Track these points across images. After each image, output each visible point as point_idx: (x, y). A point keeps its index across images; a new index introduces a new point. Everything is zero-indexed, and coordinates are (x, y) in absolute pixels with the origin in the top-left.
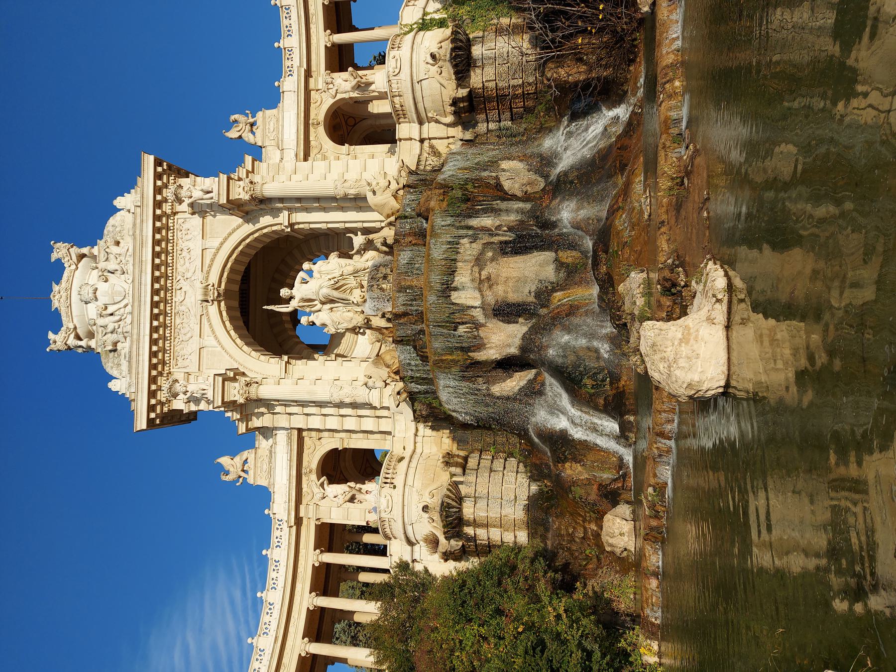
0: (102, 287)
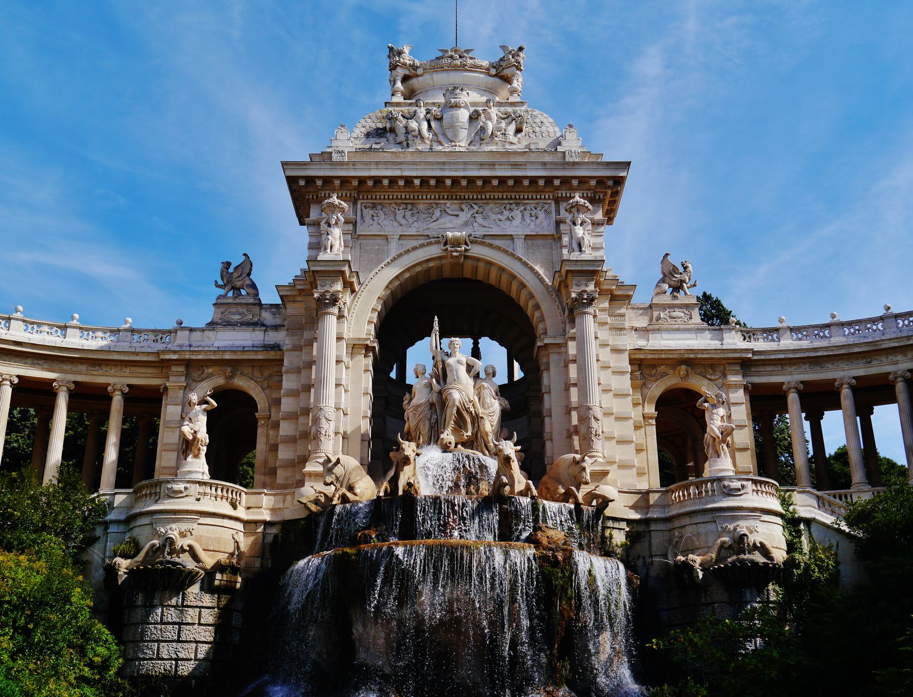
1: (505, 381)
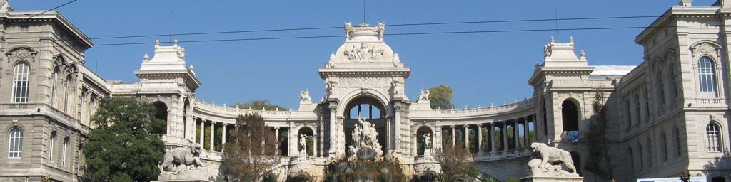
0: (367, 50)
1: (379, 117)
